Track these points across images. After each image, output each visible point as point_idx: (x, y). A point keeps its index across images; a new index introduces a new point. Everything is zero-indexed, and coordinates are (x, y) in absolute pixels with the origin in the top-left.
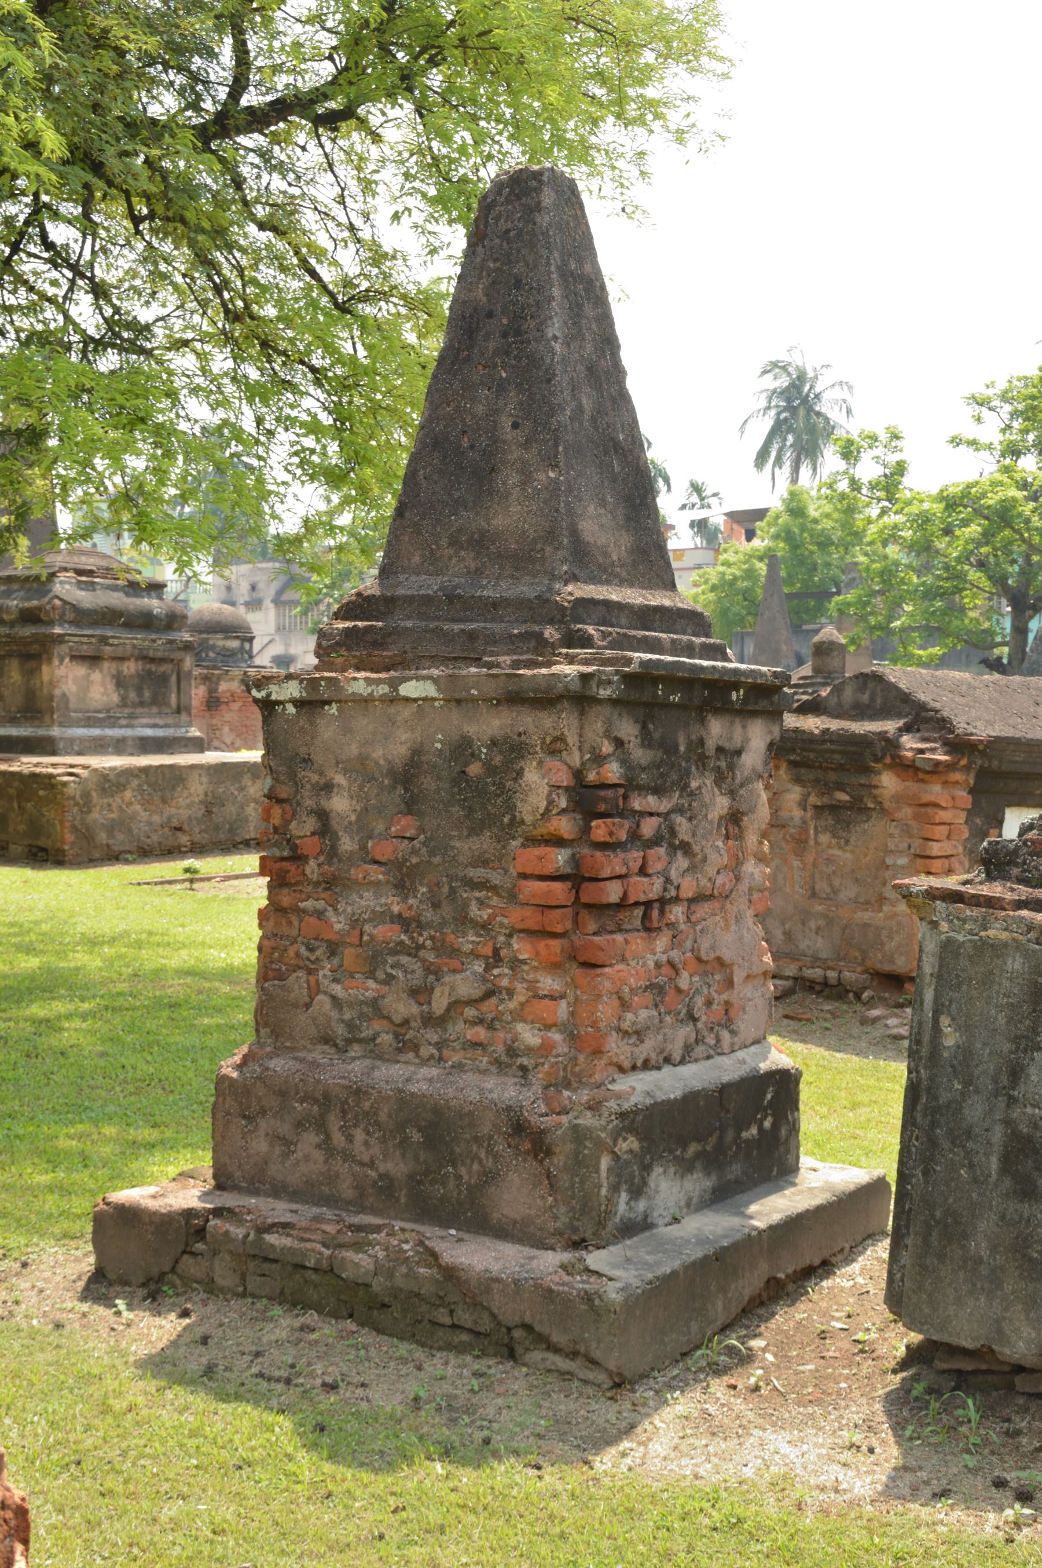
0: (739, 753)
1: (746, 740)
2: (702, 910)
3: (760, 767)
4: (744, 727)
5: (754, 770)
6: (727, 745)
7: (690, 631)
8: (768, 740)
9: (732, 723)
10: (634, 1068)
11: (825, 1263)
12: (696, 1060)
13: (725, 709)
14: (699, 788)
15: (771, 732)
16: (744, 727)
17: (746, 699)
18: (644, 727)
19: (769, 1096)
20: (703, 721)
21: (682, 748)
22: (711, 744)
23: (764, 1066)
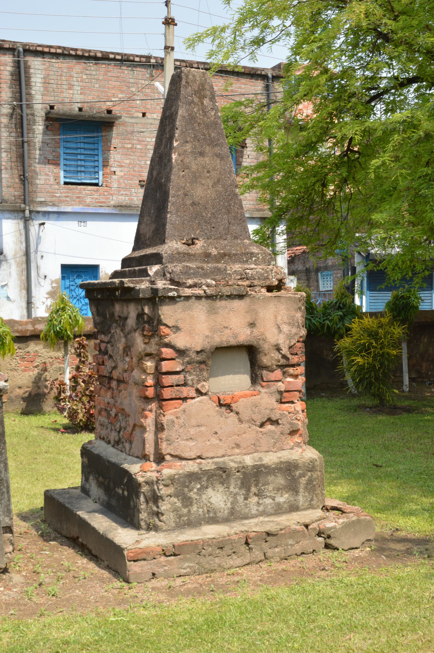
0: (126, 318)
1: (129, 313)
2: (122, 386)
3: (134, 326)
4: (127, 307)
5: (132, 327)
6: (122, 315)
7: (134, 264)
8: (137, 313)
9: (123, 305)
10: (103, 439)
11: (96, 557)
12: (118, 449)
13: (118, 300)
14: (113, 333)
15: (137, 309)
16: (127, 307)
17: (121, 294)
18: (97, 309)
19: (126, 480)
20: (113, 305)
21: (108, 316)
22: (116, 314)
23: (126, 466)
